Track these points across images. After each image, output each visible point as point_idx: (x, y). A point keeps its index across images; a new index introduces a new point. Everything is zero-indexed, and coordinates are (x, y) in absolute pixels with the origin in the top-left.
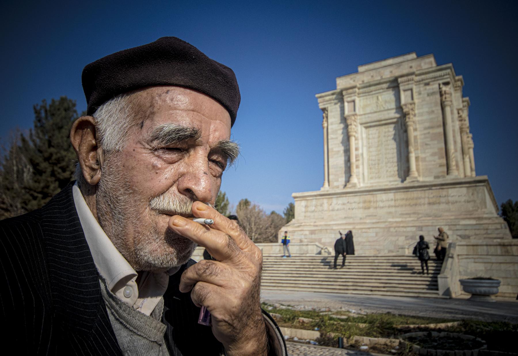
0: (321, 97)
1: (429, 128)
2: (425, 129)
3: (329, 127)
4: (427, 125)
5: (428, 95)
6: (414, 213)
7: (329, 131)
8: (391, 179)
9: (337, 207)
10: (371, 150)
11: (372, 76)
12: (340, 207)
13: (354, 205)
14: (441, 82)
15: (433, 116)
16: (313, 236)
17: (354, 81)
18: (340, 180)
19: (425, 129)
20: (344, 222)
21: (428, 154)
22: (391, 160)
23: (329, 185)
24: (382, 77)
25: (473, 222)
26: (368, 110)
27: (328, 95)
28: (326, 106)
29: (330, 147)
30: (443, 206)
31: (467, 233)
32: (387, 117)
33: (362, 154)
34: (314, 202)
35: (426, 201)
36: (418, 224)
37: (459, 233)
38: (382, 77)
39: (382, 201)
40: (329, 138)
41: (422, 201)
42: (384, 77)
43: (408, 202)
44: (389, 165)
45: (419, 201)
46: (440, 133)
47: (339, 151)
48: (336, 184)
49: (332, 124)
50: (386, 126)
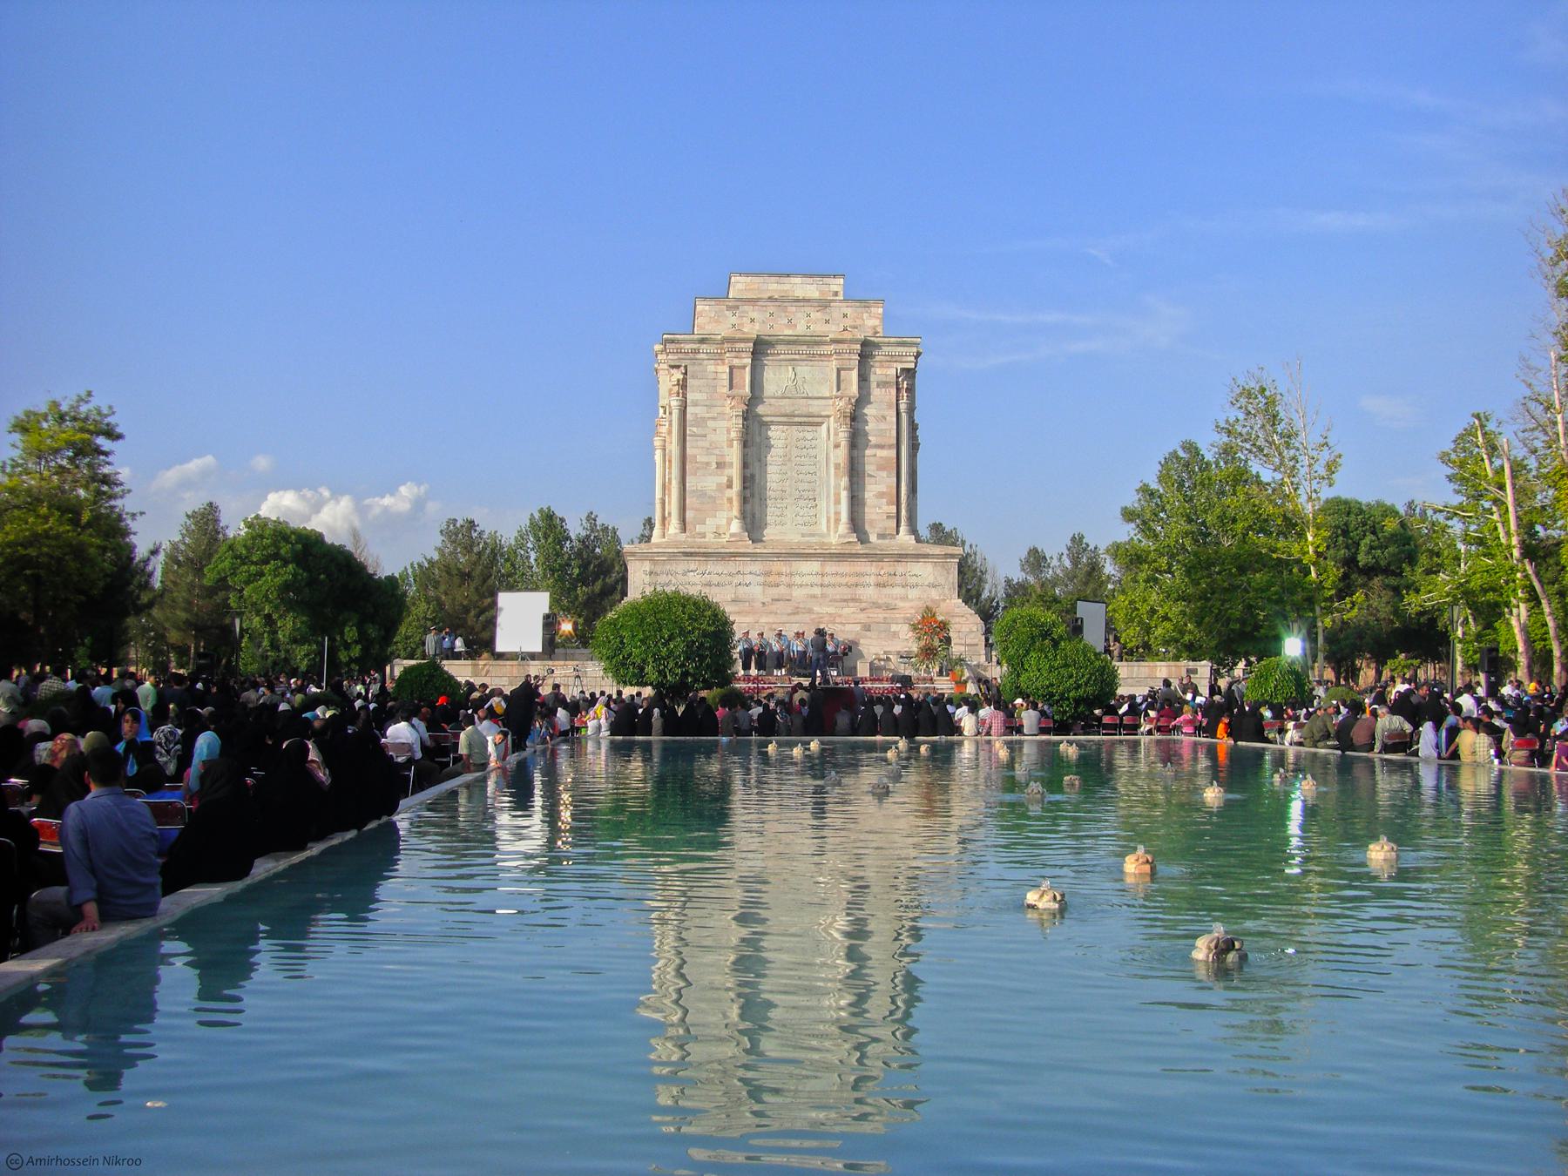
0: (673, 341)
6: (853, 600)
7: (689, 417)
8: (805, 530)
13: (748, 579)
14: (900, 366)
15: (883, 426)
22: (806, 494)
23: (684, 530)
27: (693, 341)
29: (689, 451)
30: (898, 591)
32: (804, 410)
33: (753, 476)
35: (872, 580)
36: (862, 617)
41: (868, 580)
43: (844, 580)
44: (801, 503)
45: (862, 580)
47: (708, 464)
48: (699, 528)
49: (695, 404)
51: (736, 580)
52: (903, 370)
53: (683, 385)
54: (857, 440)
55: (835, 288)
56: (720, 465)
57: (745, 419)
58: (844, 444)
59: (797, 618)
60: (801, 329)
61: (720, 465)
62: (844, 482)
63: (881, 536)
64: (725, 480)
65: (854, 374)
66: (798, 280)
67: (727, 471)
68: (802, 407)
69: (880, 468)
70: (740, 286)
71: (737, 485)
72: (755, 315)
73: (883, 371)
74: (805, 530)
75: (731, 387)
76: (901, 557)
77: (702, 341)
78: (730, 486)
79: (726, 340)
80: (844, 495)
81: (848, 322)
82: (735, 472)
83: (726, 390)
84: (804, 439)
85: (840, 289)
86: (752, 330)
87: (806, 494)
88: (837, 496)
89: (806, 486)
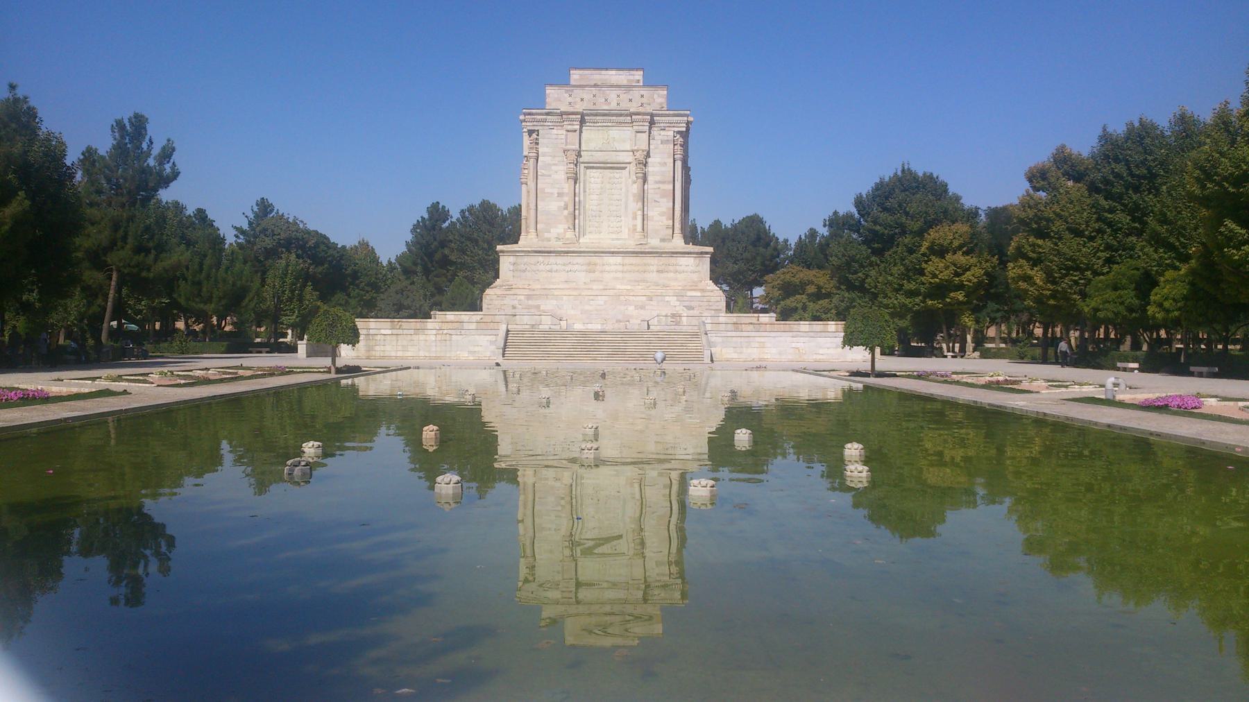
0: (530, 114)
1: (659, 182)
4: (658, 178)
6: (644, 281)
8: (614, 236)
9: (555, 267)
12: (559, 267)
15: (663, 169)
16: (530, 302)
20: (566, 286)
25: (699, 294)
26: (592, 146)
30: (671, 275)
31: (693, 304)
34: (526, 259)
35: (654, 268)
37: (686, 304)
39: (609, 265)
43: (636, 268)
48: (546, 235)
51: (567, 268)
52: (679, 132)
55: (637, 77)
56: (560, 195)
59: (607, 292)
60: (613, 105)
61: (560, 195)
63: (663, 240)
64: (562, 204)
66: (614, 72)
67: (566, 199)
68: (613, 157)
69: (663, 196)
70: (575, 76)
71: (571, 208)
72: (585, 96)
74: (614, 236)
76: (674, 254)
77: (547, 114)
78: (566, 208)
80: (640, 213)
81: (644, 100)
82: (568, 199)
85: (641, 78)
86: (579, 107)
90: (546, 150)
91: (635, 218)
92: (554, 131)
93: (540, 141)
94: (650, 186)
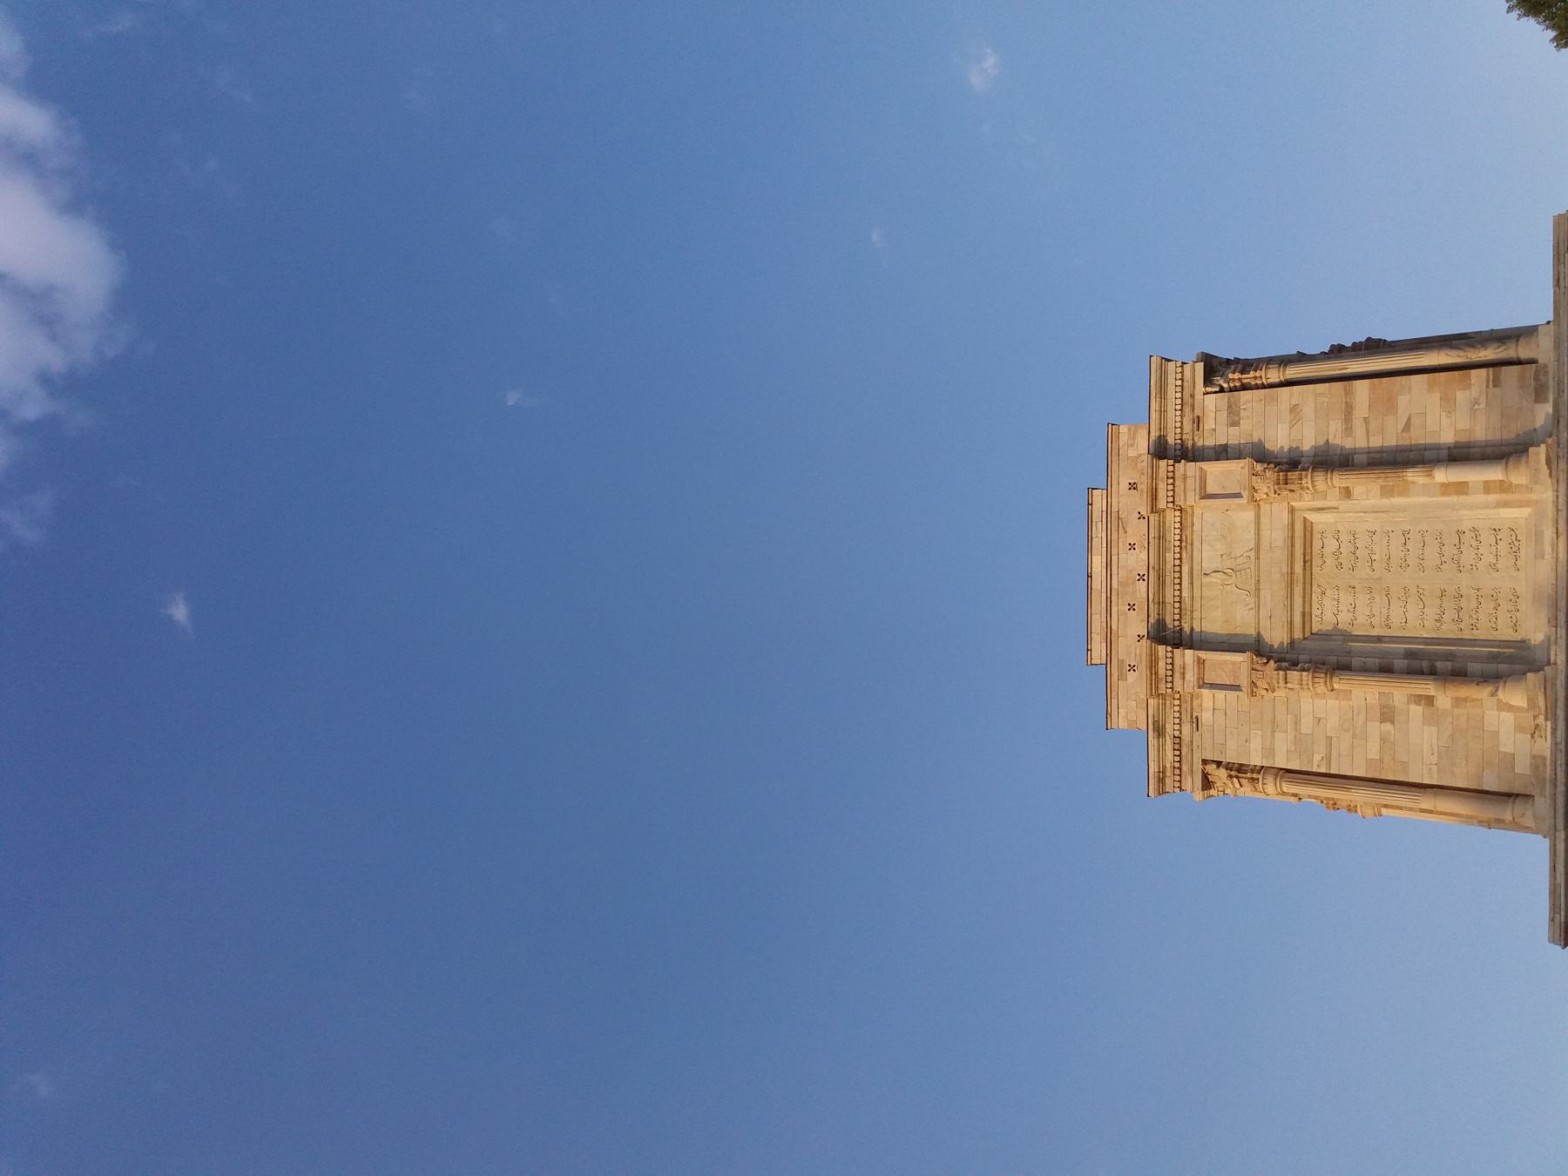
0: (1161, 780)
2: (1348, 430)
3: (1281, 763)
5: (1235, 424)
10: (1396, 619)
11: (1132, 607)
15: (1308, 411)
17: (1132, 668)
18: (1509, 749)
19: (1348, 430)
21: (1445, 422)
22: (1449, 551)
23: (1528, 797)
24: (1141, 577)
27: (1161, 750)
28: (1198, 766)
32: (1281, 555)
33: (1410, 655)
38: (1141, 577)
40: (1323, 770)
42: (1143, 571)
44: (1468, 557)
46: (1372, 389)
47: (1383, 740)
49: (1270, 751)
50: (1317, 561)
52: (1208, 381)
53: (1239, 770)
54: (1331, 461)
56: (1387, 715)
57: (1294, 664)
58: (1339, 480)
62: (1414, 476)
64: (1416, 710)
65: (1214, 469)
69: (1390, 406)
71: (1429, 688)
73: (1215, 417)
75: (1236, 688)
77: (1160, 731)
78: (1430, 701)
79: (1154, 691)
80: (1442, 475)
82: (1399, 692)
83: (1243, 695)
84: (1337, 553)
87: (1449, 551)
88: (1446, 489)
89: (1432, 553)
90: (1256, 744)
91: (1461, 488)
92: (1206, 717)
93: (1231, 757)
94: (1358, 440)
